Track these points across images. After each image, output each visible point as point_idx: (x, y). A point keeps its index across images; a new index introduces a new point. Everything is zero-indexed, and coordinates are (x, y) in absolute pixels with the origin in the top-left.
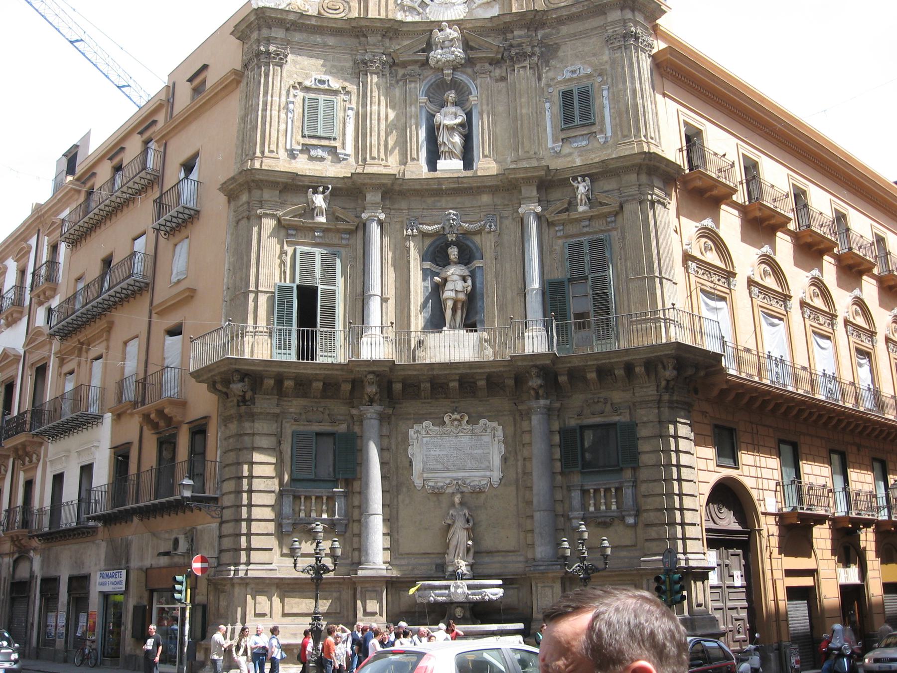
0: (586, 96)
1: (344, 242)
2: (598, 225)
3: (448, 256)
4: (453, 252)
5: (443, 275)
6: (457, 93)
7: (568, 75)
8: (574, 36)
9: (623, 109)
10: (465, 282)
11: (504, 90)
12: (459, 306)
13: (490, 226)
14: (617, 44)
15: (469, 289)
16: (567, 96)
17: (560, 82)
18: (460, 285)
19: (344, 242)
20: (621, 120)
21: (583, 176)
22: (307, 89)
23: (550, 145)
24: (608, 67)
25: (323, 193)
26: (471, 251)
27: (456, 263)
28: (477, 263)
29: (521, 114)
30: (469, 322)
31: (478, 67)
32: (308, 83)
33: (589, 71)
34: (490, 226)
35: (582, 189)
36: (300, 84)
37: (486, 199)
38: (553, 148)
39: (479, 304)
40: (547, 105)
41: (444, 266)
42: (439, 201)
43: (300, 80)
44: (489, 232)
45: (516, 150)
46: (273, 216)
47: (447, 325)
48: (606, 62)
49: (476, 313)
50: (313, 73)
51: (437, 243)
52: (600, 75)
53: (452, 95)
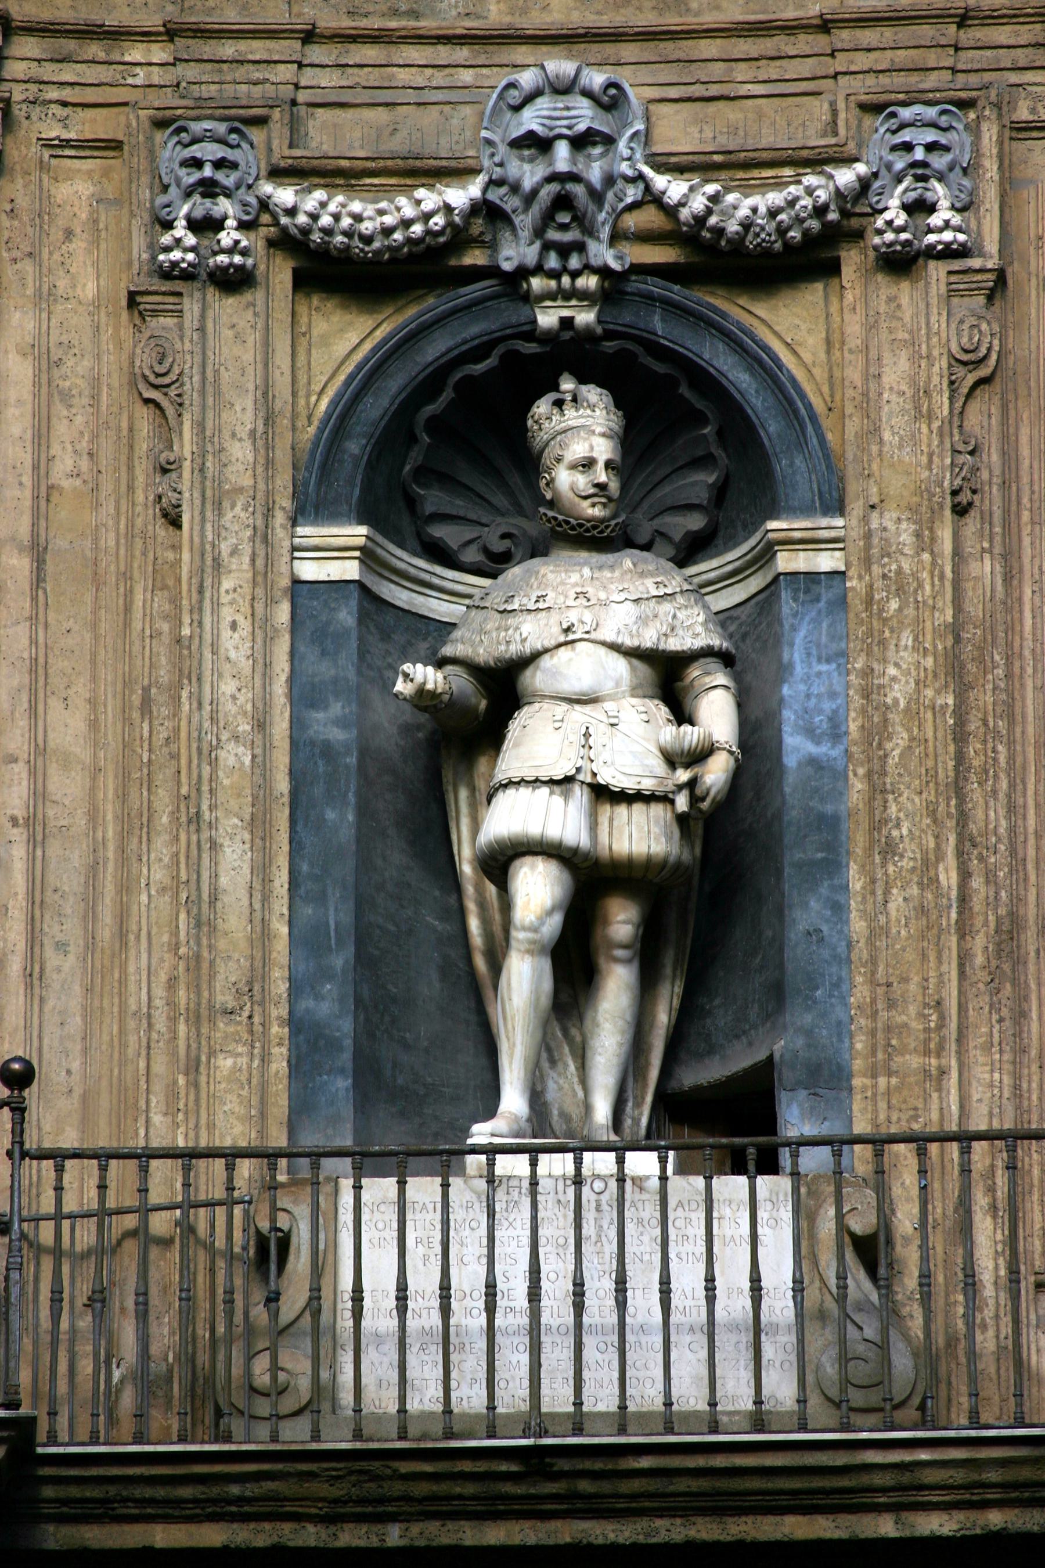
3: (528, 462)
5: (484, 641)
10: (682, 715)
12: (622, 920)
13: (920, 208)
15: (716, 773)
18: (632, 743)
26: (738, 429)
28: (808, 547)
30: (695, 1076)
34: (920, 208)
39: (807, 914)
41: (494, 564)
47: (513, 1100)
49: (777, 996)
51: (436, 348)
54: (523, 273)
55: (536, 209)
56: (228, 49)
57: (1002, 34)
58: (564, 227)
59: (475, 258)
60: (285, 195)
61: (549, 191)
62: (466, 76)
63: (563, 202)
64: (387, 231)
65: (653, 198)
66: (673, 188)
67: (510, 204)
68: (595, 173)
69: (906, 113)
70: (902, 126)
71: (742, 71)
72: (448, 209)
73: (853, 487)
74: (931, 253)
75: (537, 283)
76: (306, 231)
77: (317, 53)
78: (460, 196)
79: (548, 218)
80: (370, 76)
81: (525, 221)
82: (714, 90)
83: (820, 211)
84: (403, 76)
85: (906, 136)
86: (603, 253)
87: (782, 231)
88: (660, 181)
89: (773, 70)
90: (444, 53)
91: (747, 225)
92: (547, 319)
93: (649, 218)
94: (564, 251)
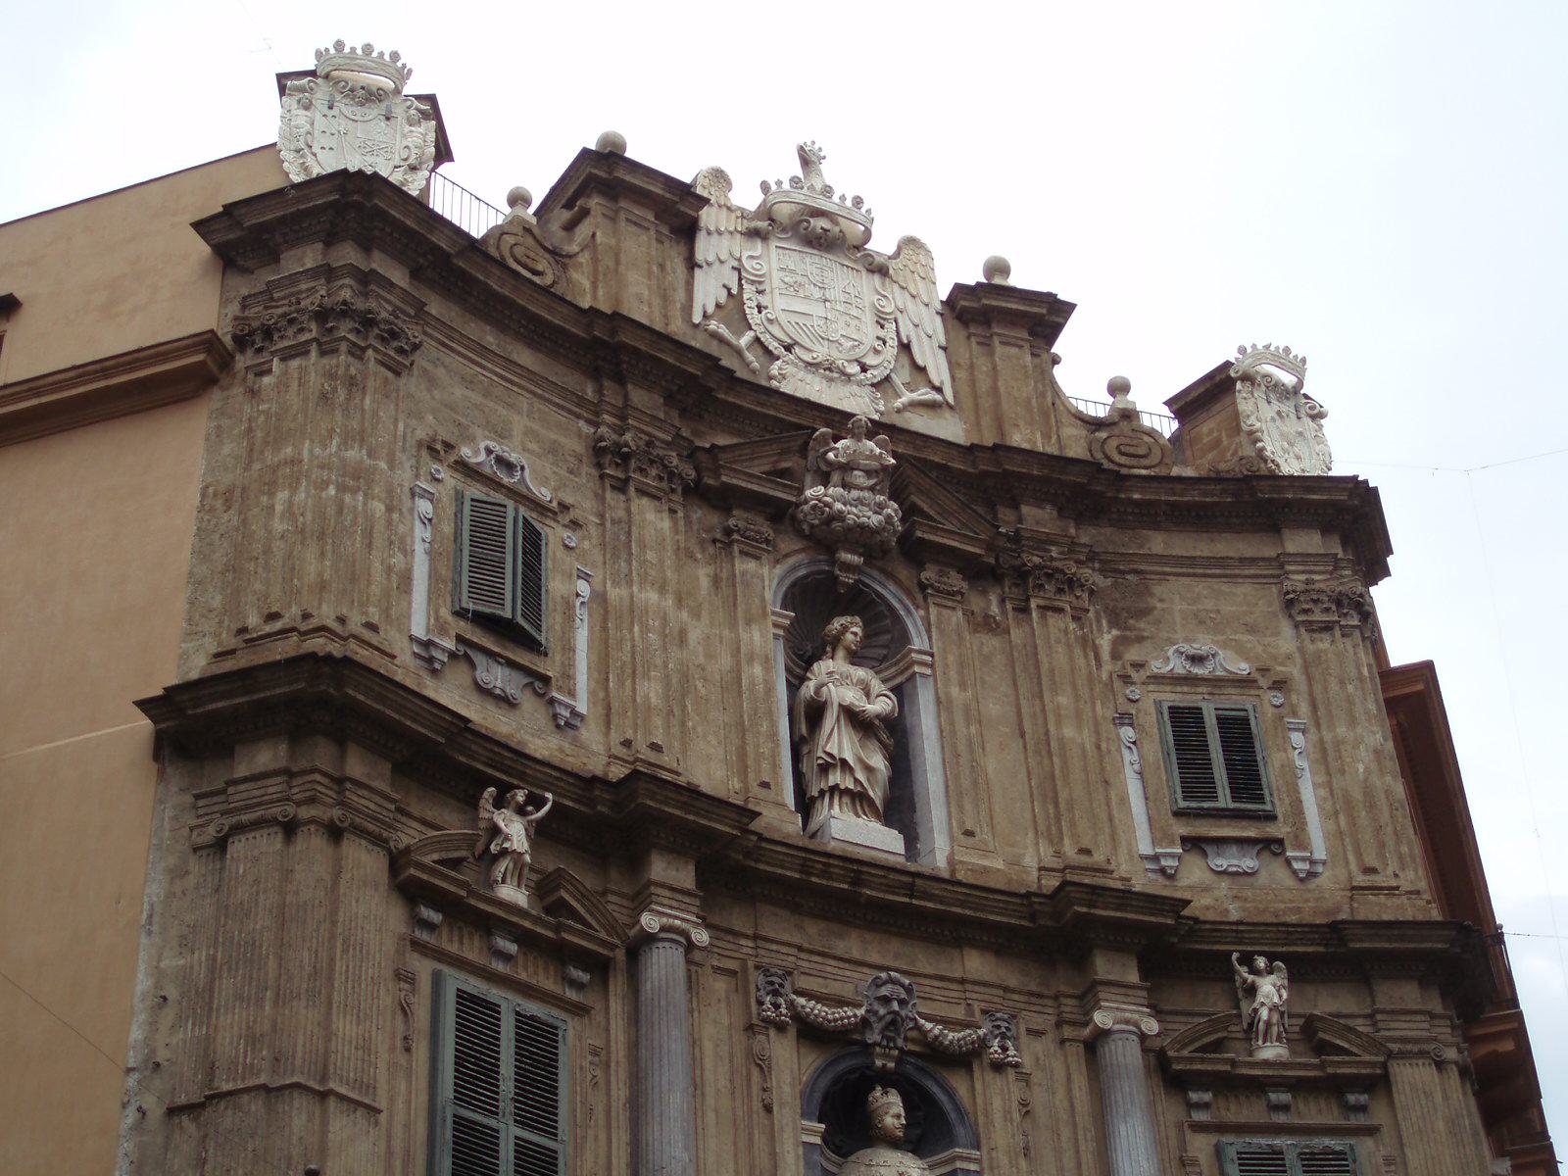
0: (1238, 733)
1: (571, 994)
2: (1317, 1112)
4: (891, 1110)
6: (866, 625)
7: (1178, 666)
8: (1190, 566)
9: (1357, 794)
11: (999, 659)
14: (1318, 616)
16: (1185, 723)
17: (1157, 679)
19: (571, 994)
20: (1353, 821)
21: (1271, 957)
22: (463, 468)
23: (1145, 847)
24: (1295, 671)
25: (521, 811)
27: (895, 1144)
29: (1061, 740)
31: (929, 574)
32: (465, 451)
33: (1243, 668)
35: (1270, 989)
36: (449, 447)
37: (975, 964)
38: (1156, 858)
40: (1127, 733)
42: (841, 937)
43: (444, 434)
44: (998, 1067)
45: (1056, 840)
46: (378, 841)
48: (1289, 657)
50: (479, 432)
52: (1279, 685)
53: (851, 629)
54: (875, 1044)
55: (883, 1023)
56: (774, 947)
57: (1016, 997)
58: (891, 1031)
59: (857, 1037)
60: (802, 1001)
61: (889, 1018)
62: (848, 973)
63: (893, 1022)
64: (835, 1020)
65: (918, 1028)
66: (929, 1026)
67: (873, 1019)
68: (903, 1013)
69: (998, 1015)
70: (997, 1020)
71: (936, 991)
72: (855, 1016)
73: (984, 1142)
74: (1010, 1064)
75: (878, 1049)
76: (808, 1015)
77: (803, 955)
78: (861, 1012)
79: (886, 1027)
80: (819, 967)
81: (877, 1027)
82: (927, 995)
83: (973, 1043)
84: (829, 969)
85: (999, 1023)
86: (900, 1042)
87: (960, 1047)
88: (922, 1021)
89: (946, 993)
90: (841, 965)
91: (951, 1042)
92: (879, 1063)
93: (914, 1034)
94: (889, 1039)
